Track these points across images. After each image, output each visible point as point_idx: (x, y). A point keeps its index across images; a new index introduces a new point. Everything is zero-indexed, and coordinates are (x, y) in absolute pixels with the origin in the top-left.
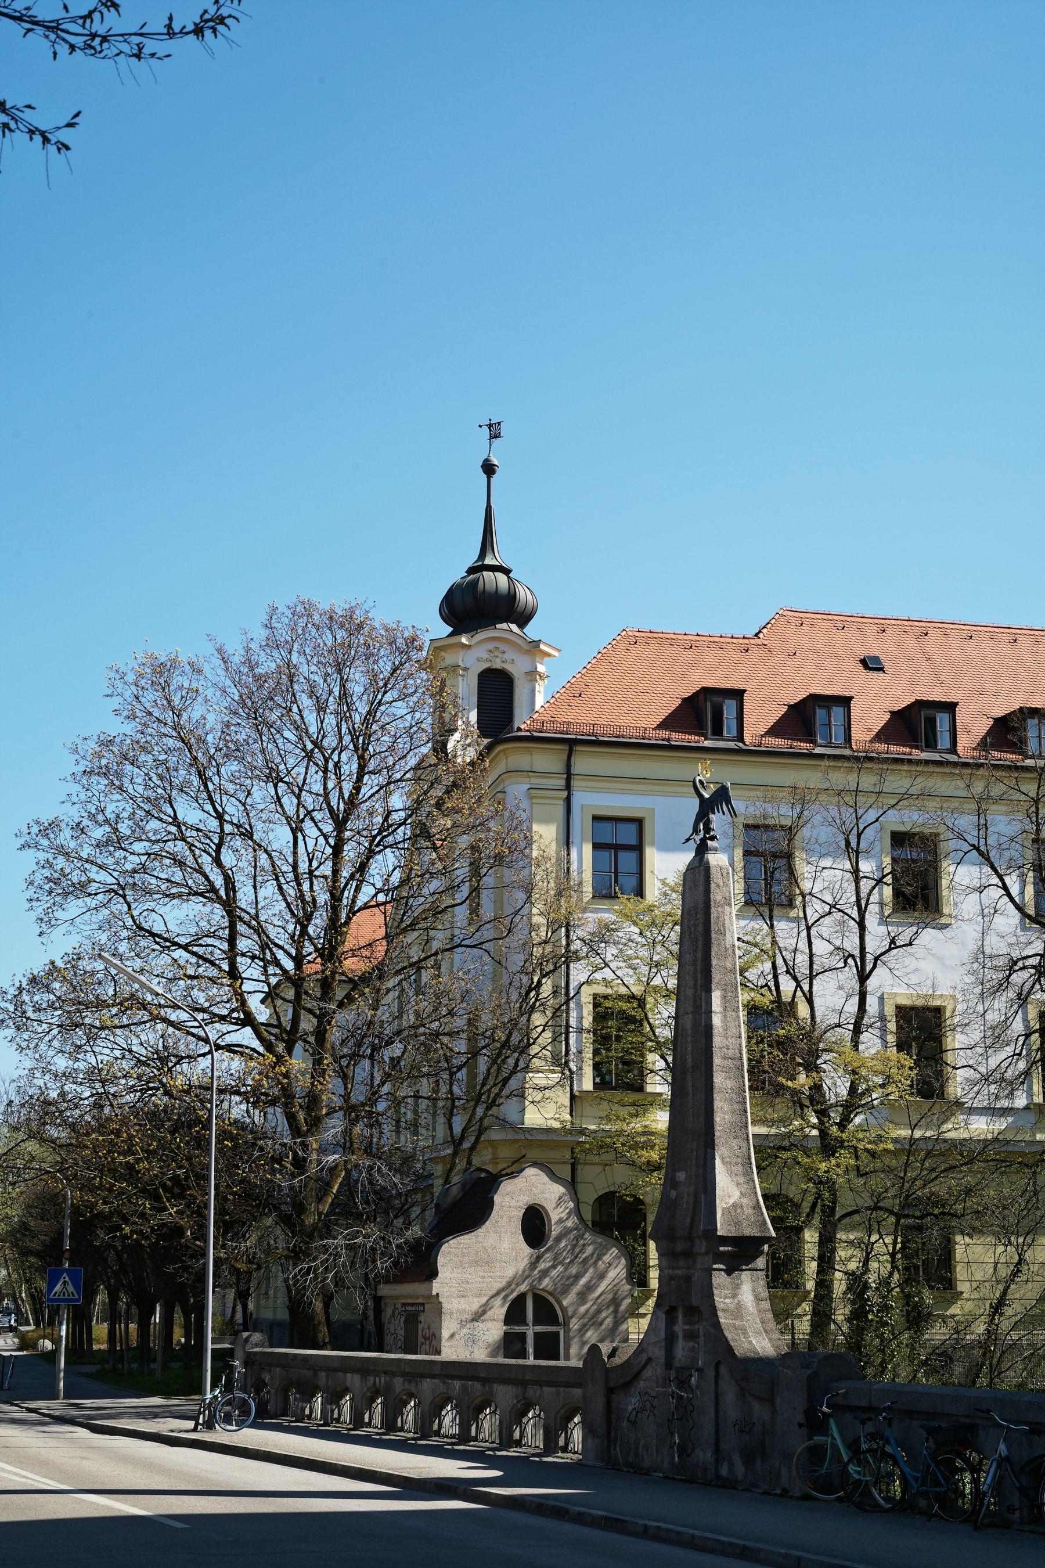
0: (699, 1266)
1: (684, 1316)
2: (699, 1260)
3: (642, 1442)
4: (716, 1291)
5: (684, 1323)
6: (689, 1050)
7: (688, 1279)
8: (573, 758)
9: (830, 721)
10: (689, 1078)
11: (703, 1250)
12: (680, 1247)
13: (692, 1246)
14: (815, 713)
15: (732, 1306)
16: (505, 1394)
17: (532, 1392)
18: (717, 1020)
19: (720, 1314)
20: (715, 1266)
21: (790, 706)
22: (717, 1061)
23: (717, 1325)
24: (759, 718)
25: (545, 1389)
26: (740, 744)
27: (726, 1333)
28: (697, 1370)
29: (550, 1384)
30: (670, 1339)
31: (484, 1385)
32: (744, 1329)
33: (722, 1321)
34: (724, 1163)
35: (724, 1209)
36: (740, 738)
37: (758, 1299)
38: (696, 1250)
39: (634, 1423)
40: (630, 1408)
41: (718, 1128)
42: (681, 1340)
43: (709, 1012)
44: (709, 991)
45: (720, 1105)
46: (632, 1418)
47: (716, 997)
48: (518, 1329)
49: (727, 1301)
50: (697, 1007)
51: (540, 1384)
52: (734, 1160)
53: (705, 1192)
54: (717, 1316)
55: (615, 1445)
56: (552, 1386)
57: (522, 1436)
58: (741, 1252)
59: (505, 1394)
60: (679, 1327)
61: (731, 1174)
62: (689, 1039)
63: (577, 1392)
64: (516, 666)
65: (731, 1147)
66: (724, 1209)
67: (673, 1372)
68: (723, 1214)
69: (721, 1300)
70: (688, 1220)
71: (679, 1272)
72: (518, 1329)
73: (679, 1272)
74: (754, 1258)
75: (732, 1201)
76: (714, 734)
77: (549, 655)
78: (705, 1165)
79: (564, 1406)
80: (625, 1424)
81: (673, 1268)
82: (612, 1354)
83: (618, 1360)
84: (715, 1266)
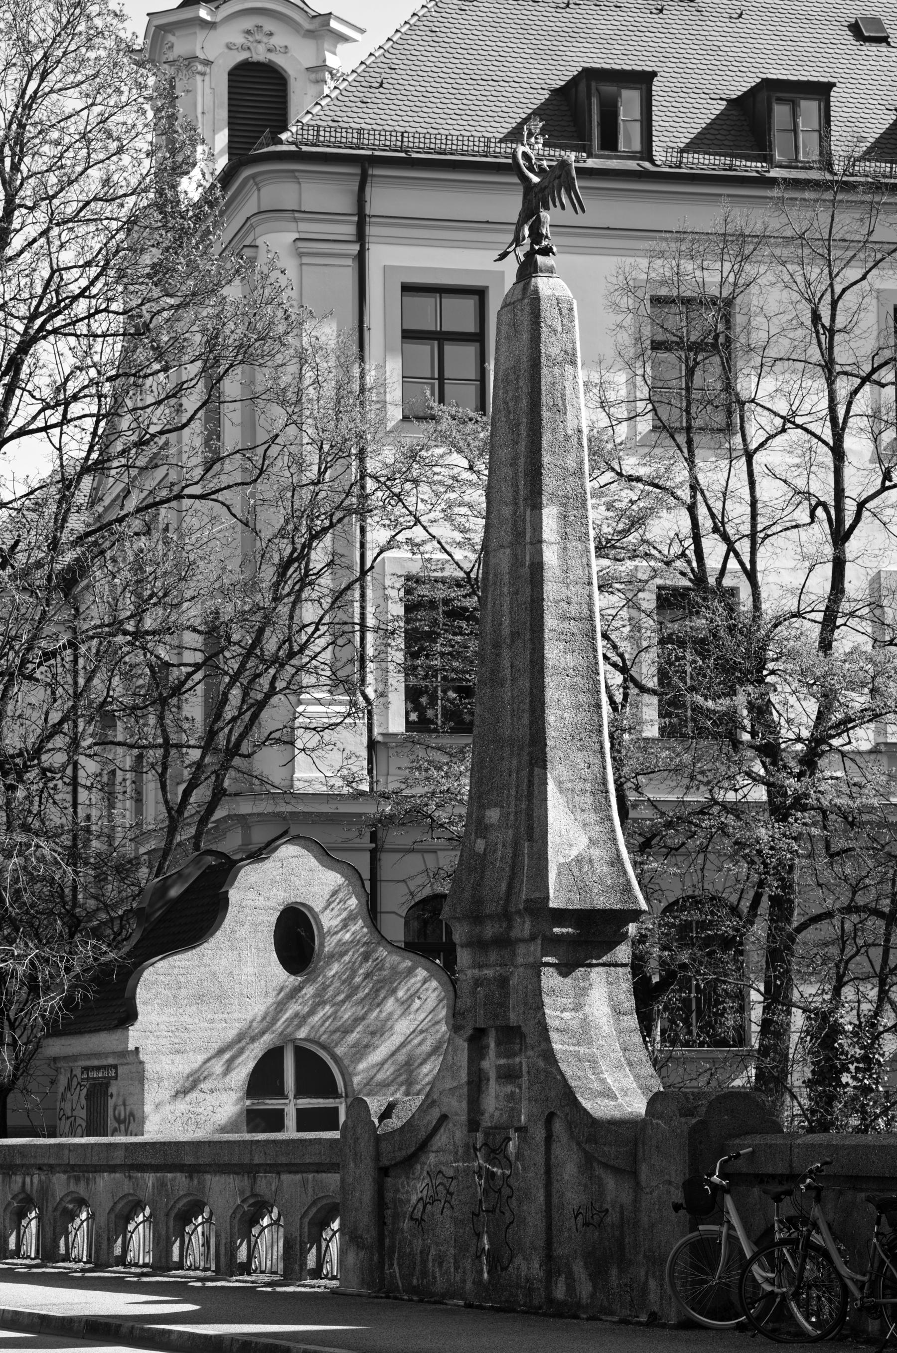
0: (520, 960)
1: (498, 1044)
2: (521, 950)
3: (433, 1252)
4: (547, 1000)
5: (499, 1056)
6: (506, 607)
7: (503, 982)
8: (368, 189)
9: (795, 124)
10: (506, 653)
11: (527, 933)
12: (489, 931)
13: (510, 927)
14: (770, 110)
15: (574, 1025)
16: (223, 1192)
17: (265, 1185)
18: (550, 556)
19: (554, 1036)
20: (546, 959)
21: (730, 101)
22: (550, 622)
23: (549, 1056)
24: (679, 119)
25: (285, 1177)
26: (647, 165)
27: (563, 1067)
28: (518, 1129)
29: (292, 1168)
30: (476, 1084)
31: (191, 1178)
32: (593, 1062)
33: (556, 1047)
34: (561, 790)
35: (560, 866)
36: (647, 153)
37: (617, 1012)
38: (515, 933)
39: (419, 1222)
40: (414, 1198)
41: (552, 735)
42: (492, 1082)
43: (538, 541)
44: (537, 506)
45: (556, 696)
46: (418, 1215)
47: (550, 516)
48: (272, 1104)
49: (566, 1015)
50: (518, 535)
51: (277, 1169)
52: (579, 786)
53: (530, 839)
54: (548, 1040)
55: (391, 1259)
56: (296, 1172)
57: (250, 1256)
58: (590, 935)
59: (223, 1192)
60: (491, 1063)
61: (573, 808)
62: (505, 590)
63: (333, 1179)
64: (293, 56)
65: (574, 765)
66: (560, 866)
67: (480, 1136)
68: (559, 874)
69: (557, 1013)
70: (504, 885)
71: (489, 972)
72: (272, 1104)
73: (489, 972)
74: (611, 945)
75: (574, 853)
76: (603, 147)
77: (345, 39)
78: (530, 794)
79: (314, 1203)
80: (406, 1225)
81: (480, 967)
82: (386, 1114)
83: (395, 1123)
84: (546, 959)
